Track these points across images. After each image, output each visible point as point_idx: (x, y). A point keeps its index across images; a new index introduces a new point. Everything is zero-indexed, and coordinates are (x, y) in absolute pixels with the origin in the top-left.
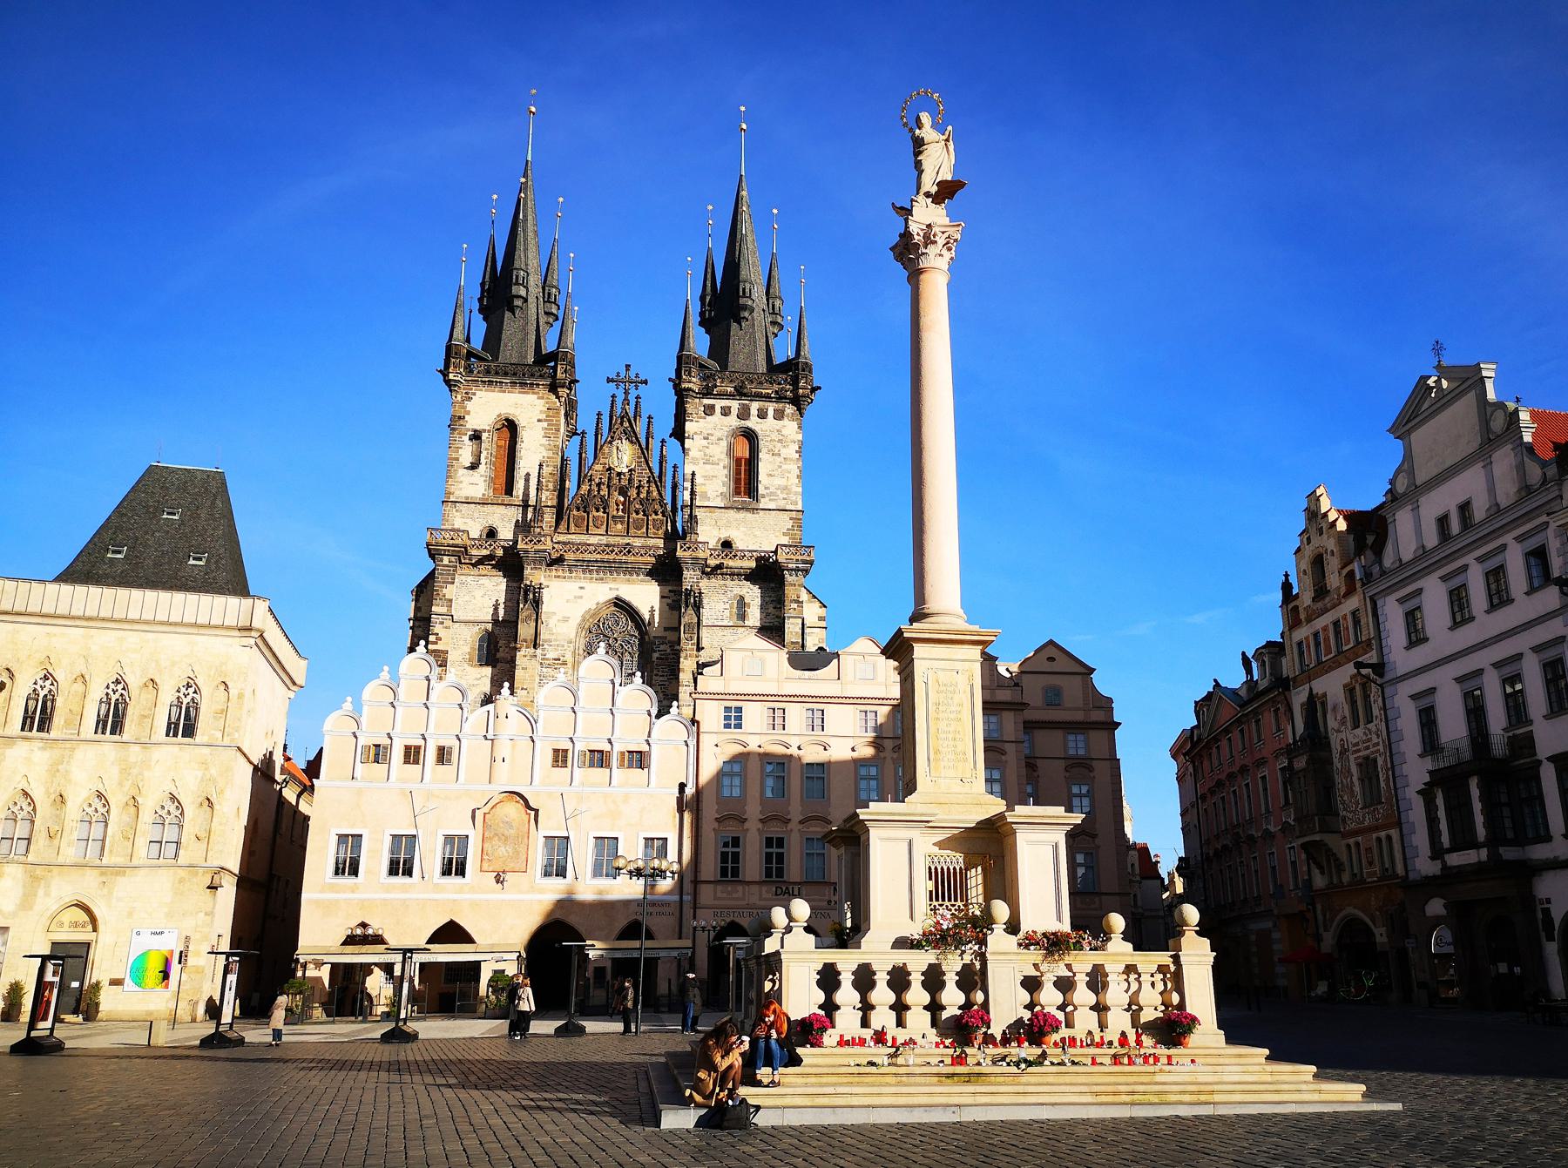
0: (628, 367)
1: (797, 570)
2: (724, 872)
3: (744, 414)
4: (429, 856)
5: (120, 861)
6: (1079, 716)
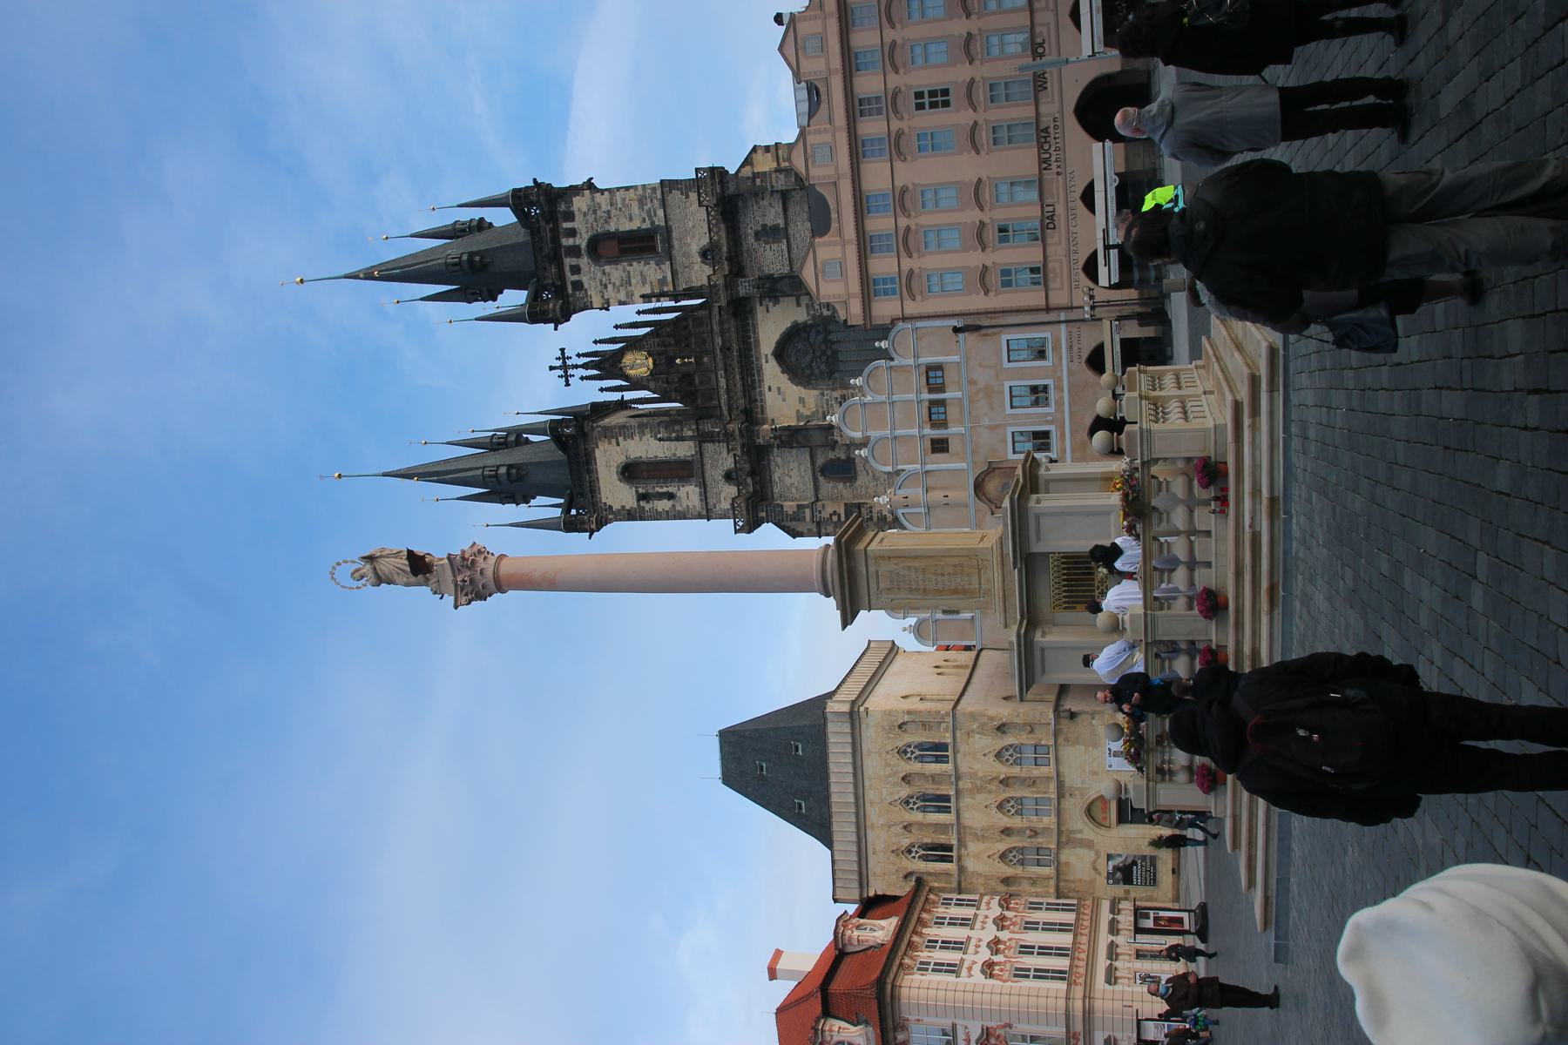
0: (551, 368)
1: (721, 183)
3: (575, 251)
5: (1053, 786)
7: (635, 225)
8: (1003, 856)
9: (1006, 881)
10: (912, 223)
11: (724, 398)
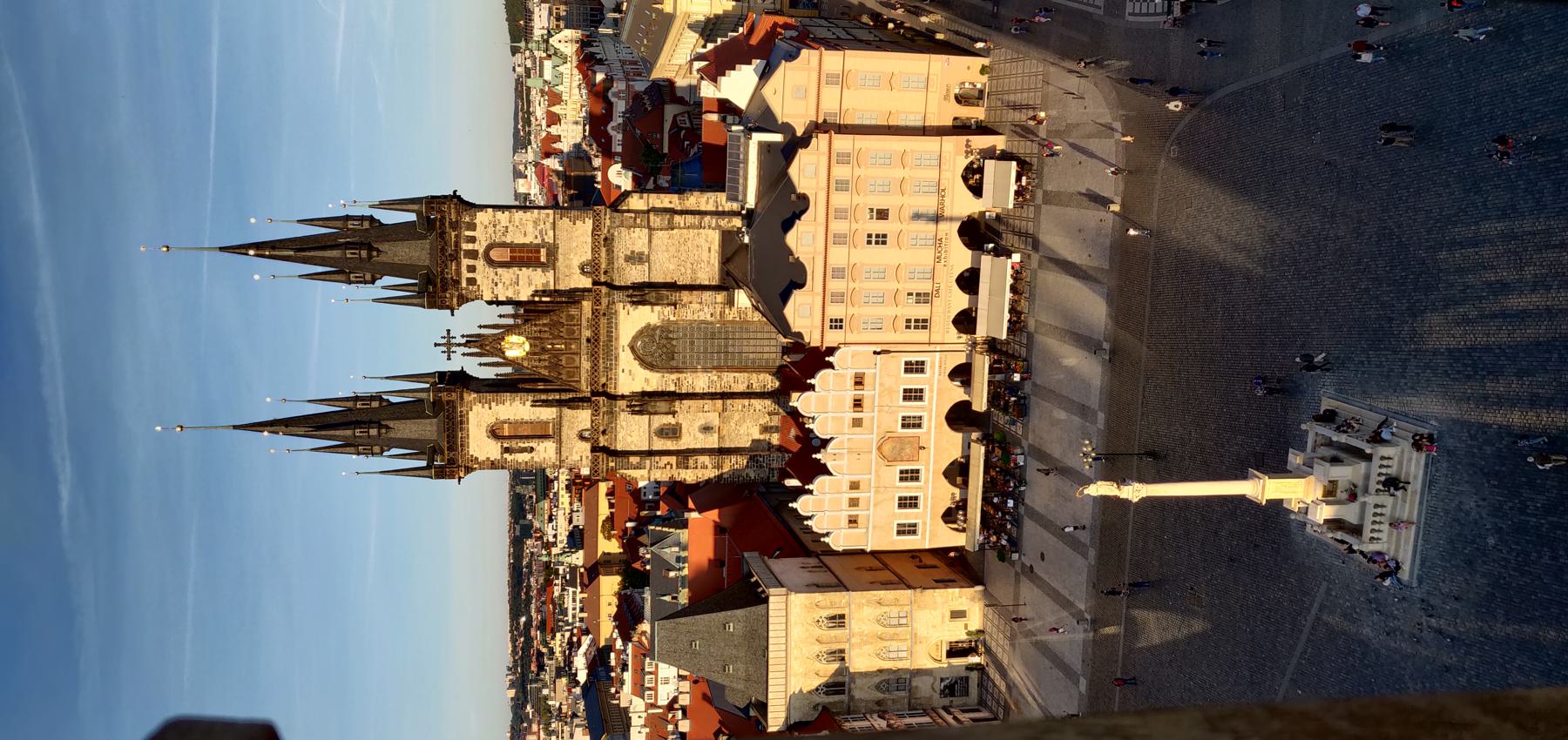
2: (924, 327)
3: (473, 254)
4: (909, 489)
6: (815, 75)
7: (527, 241)
8: (878, 687)
9: (879, 703)
10: (857, 285)
11: (584, 376)
